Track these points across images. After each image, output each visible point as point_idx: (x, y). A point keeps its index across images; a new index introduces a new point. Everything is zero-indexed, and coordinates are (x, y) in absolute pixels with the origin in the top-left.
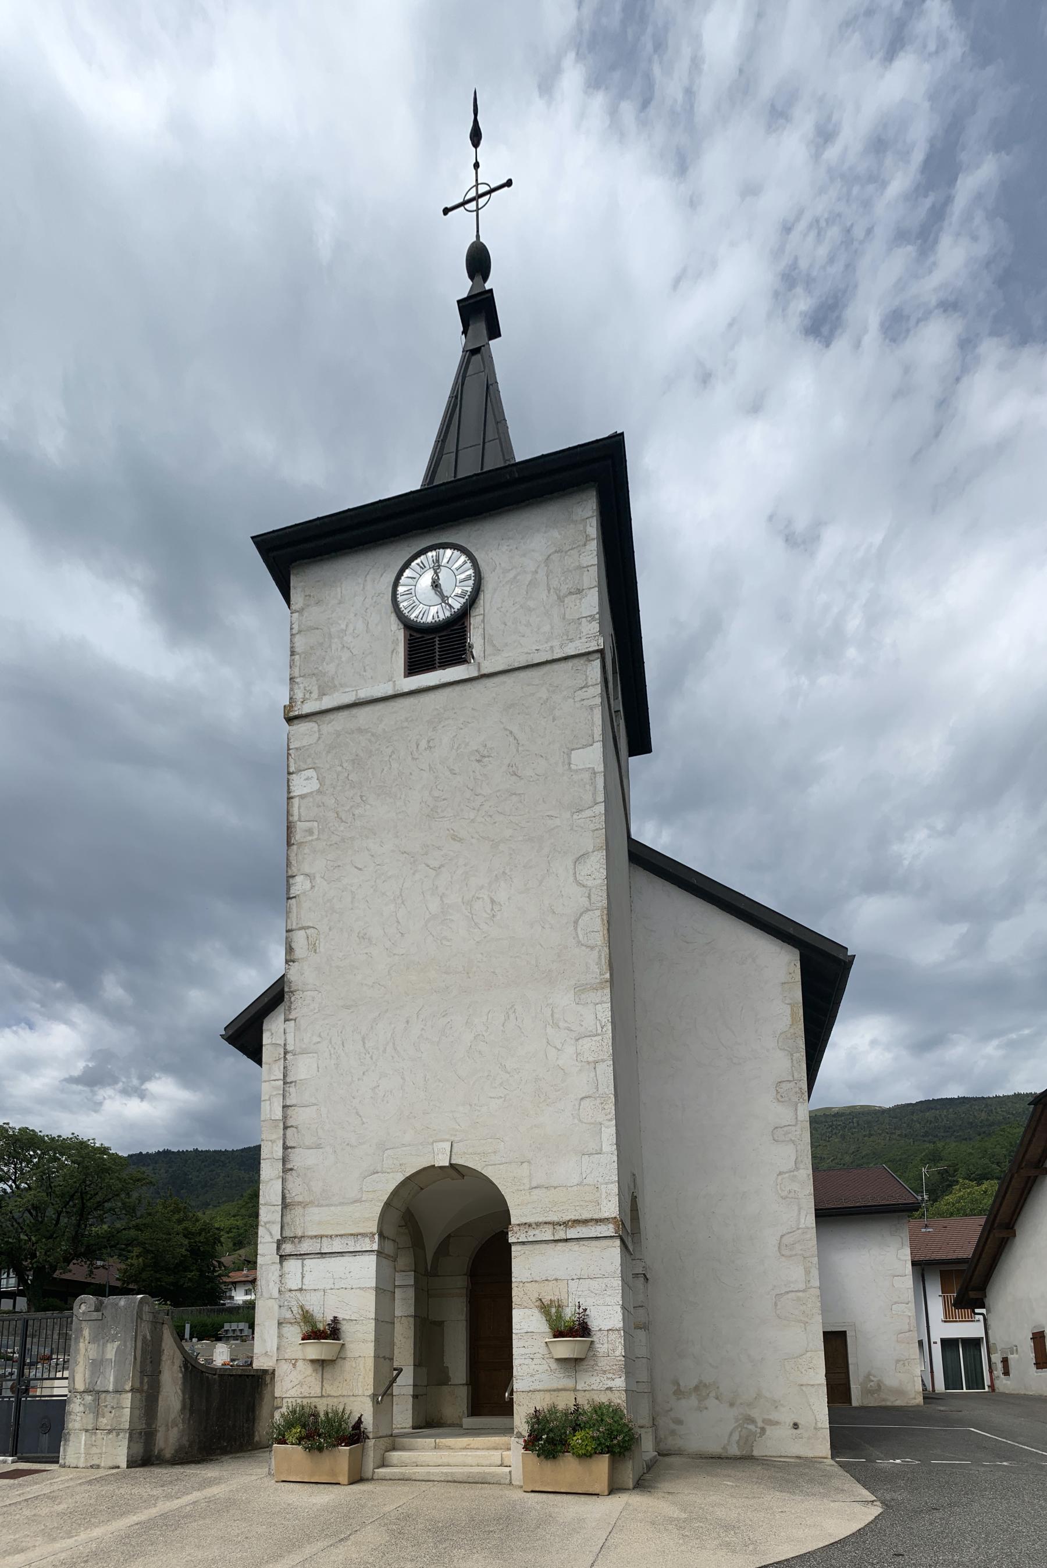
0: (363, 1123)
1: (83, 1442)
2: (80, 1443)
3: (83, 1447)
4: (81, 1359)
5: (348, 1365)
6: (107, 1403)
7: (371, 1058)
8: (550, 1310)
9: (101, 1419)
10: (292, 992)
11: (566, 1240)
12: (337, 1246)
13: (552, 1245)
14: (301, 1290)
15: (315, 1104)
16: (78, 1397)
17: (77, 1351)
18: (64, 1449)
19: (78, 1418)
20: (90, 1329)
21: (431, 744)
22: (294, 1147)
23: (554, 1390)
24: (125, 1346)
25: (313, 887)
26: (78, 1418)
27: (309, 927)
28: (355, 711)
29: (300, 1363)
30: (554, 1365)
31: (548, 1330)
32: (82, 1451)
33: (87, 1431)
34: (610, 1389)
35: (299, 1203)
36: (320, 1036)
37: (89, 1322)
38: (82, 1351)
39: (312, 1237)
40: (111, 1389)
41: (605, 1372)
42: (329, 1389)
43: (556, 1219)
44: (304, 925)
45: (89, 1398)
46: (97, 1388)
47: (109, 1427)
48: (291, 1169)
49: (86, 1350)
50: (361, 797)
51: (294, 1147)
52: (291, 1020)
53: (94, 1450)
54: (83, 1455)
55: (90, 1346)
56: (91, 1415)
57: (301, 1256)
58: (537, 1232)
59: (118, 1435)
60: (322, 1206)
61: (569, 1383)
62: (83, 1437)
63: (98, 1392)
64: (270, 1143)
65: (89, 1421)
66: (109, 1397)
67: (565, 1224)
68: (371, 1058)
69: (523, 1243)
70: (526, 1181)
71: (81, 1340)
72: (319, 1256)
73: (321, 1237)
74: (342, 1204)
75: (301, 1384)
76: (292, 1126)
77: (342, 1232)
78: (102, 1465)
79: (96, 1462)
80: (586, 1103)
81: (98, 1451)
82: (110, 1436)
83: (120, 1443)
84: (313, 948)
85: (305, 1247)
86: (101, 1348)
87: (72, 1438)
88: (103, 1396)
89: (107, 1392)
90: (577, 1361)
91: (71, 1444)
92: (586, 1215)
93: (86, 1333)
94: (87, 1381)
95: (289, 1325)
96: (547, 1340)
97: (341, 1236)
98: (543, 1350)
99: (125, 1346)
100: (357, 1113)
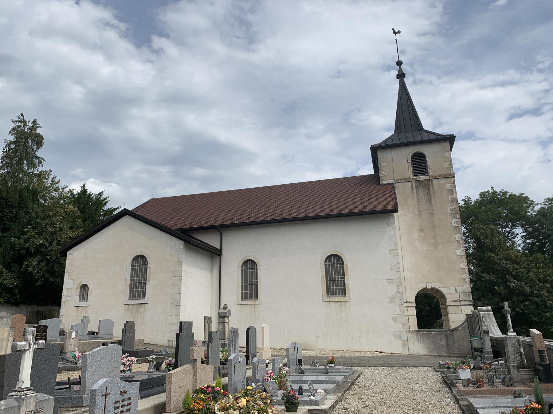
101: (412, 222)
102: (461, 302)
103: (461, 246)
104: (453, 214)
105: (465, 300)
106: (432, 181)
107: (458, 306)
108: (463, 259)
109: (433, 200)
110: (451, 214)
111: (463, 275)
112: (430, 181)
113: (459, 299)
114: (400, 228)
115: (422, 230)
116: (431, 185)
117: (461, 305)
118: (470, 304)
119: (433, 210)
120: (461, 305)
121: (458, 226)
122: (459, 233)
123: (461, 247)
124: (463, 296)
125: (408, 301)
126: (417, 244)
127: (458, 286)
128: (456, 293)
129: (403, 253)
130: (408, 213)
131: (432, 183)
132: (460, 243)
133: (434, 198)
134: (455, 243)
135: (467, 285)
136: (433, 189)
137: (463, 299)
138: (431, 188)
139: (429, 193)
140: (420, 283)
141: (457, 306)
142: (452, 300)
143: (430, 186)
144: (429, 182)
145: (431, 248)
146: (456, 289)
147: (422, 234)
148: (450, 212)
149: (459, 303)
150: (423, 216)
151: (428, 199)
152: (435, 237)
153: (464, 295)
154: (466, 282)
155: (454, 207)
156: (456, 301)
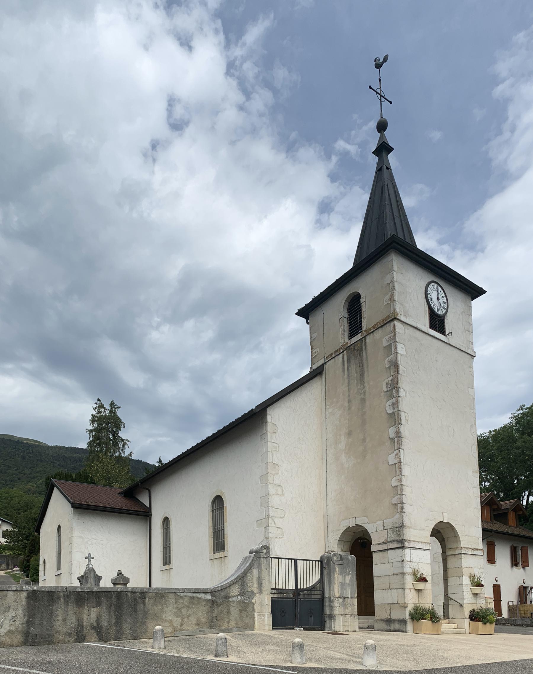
0: (425, 499)
1: (341, 620)
2: (340, 620)
3: (341, 622)
4: (336, 582)
5: (425, 592)
6: (348, 603)
7: (426, 474)
8: (472, 578)
9: (346, 610)
10: (402, 437)
11: (473, 555)
12: (420, 546)
13: (470, 556)
14: (410, 561)
15: (410, 487)
16: (337, 599)
17: (334, 578)
18: (334, 623)
19: (338, 609)
20: (339, 569)
21: (437, 359)
22: (405, 503)
23: (472, 604)
24: (353, 577)
25: (406, 396)
26: (338, 609)
27: (406, 412)
28: (415, 330)
29: (412, 590)
30: (472, 596)
31: (470, 584)
32: (341, 624)
33: (342, 615)
34: (483, 603)
35: (408, 527)
36: (411, 460)
37: (338, 565)
38: (336, 578)
39: (413, 541)
40: (349, 597)
41: (482, 598)
42: (421, 601)
43: (470, 547)
44: (404, 411)
45: (341, 600)
46: (344, 596)
47: (350, 614)
48: (405, 512)
49: (338, 578)
50: (419, 367)
51: (405, 503)
52: (402, 449)
53: (346, 624)
54: (342, 626)
55: (339, 576)
56: (343, 608)
57: (410, 548)
58: (467, 551)
59: (354, 617)
60: (414, 529)
61: (474, 601)
62: (341, 617)
63: (344, 598)
64: (272, 475)
65: (342, 611)
66: (349, 600)
67: (473, 549)
68: (426, 474)
69: (464, 554)
70: (464, 532)
71: (335, 573)
72: (415, 549)
73: (416, 542)
74: (420, 530)
75: (413, 598)
76: (404, 495)
77: (420, 541)
78: (350, 630)
79: (347, 629)
80: (476, 509)
81: (348, 624)
82: (352, 618)
83: (355, 621)
84: (407, 421)
85: (412, 545)
86: (344, 577)
87: (336, 618)
88: (346, 599)
89: (348, 598)
90: (477, 594)
91: (336, 621)
92: (476, 548)
93: (337, 570)
94: (340, 592)
95: (408, 575)
96: (471, 587)
97: (421, 542)
98: (470, 590)
99: (353, 577)
100: (423, 495)
101: (340, 422)
102: (388, 543)
103: (395, 447)
104: (389, 391)
105: (393, 541)
106: (365, 340)
107: (384, 550)
108: (396, 470)
109: (366, 374)
110: (387, 391)
111: (394, 497)
112: (364, 341)
113: (386, 540)
114: (327, 437)
115: (349, 434)
116: (364, 347)
117: (388, 549)
118: (399, 546)
119: (364, 393)
120: (388, 549)
121: (395, 411)
122: (393, 424)
123: (396, 449)
124: (392, 534)
125: (330, 551)
126: (343, 458)
127: (386, 519)
128: (384, 529)
129: (328, 476)
130: (336, 410)
131: (365, 343)
132: (394, 443)
133: (368, 370)
134: (388, 443)
135: (398, 514)
136: (366, 353)
137: (392, 539)
138: (364, 353)
139: (361, 366)
140: (344, 520)
141: (383, 552)
142: (378, 543)
143: (362, 351)
144: (362, 343)
145: (359, 460)
146: (383, 523)
147: (350, 440)
148: (385, 390)
149: (384, 547)
150: (353, 408)
151: (360, 375)
152: (364, 440)
153: (393, 532)
154: (398, 510)
155: (390, 378)
156: (383, 543)
